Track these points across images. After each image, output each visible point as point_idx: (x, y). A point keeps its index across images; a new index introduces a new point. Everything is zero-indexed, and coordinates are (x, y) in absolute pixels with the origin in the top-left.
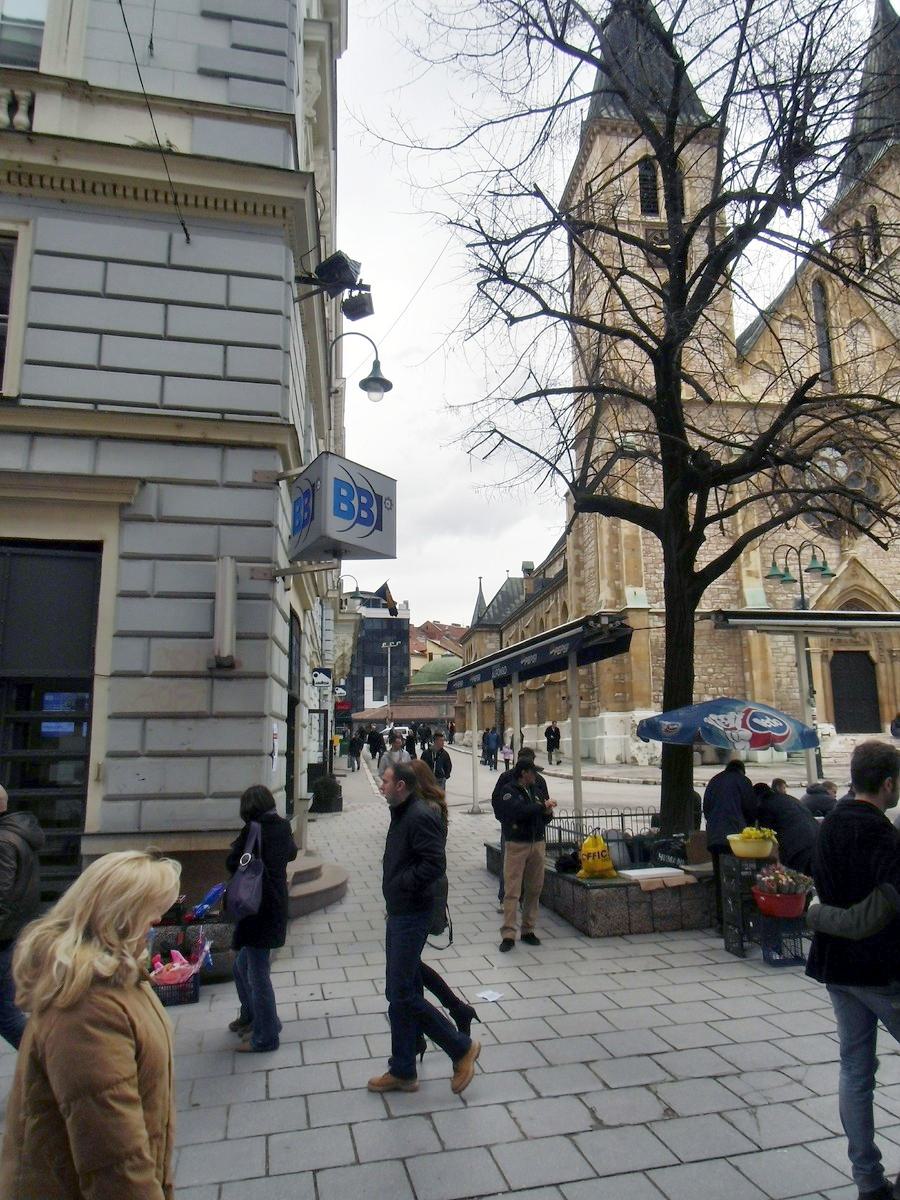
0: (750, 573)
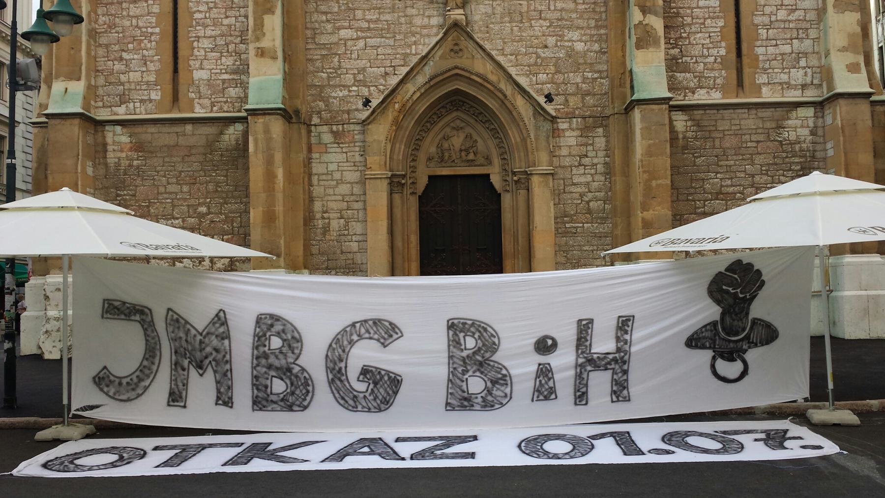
0: (262, 53)
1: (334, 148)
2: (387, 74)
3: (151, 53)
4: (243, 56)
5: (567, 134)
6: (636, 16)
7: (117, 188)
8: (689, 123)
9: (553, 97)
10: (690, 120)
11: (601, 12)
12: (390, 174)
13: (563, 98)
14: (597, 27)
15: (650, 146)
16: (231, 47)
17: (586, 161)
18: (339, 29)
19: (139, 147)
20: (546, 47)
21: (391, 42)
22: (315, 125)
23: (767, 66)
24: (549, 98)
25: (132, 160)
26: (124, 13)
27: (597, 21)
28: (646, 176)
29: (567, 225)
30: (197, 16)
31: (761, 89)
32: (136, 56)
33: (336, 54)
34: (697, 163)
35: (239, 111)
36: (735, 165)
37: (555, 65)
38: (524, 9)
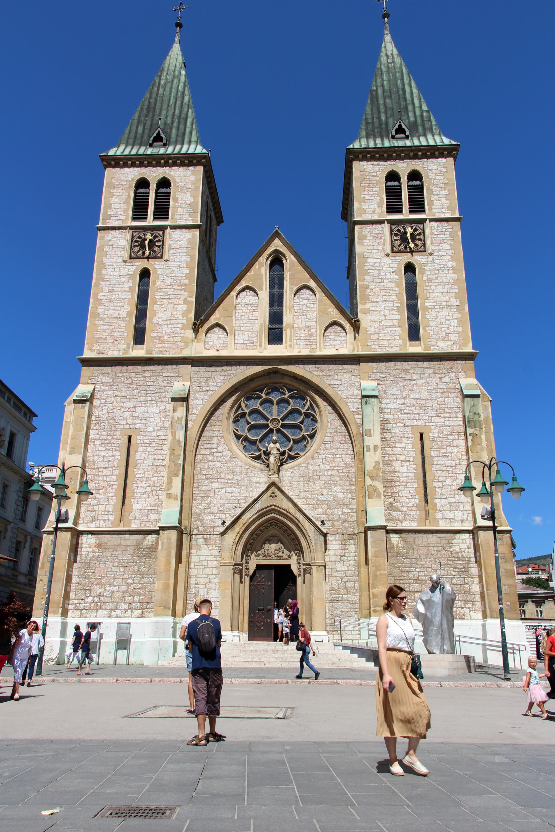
0: (169, 496)
1: (204, 548)
2: (236, 507)
3: (112, 495)
4: (160, 497)
5: (334, 542)
6: (368, 481)
7: (85, 568)
8: (400, 539)
9: (325, 522)
10: (400, 537)
11: (352, 477)
12: (234, 563)
13: (332, 522)
14: (350, 485)
15: (376, 551)
16: (154, 492)
17: (343, 558)
18: (212, 483)
19: (99, 546)
20: (322, 495)
21: (239, 490)
22: (195, 535)
23: (441, 509)
24: (323, 523)
25: (95, 552)
26: (100, 474)
27: (350, 482)
28: (374, 569)
29: (334, 596)
30: (138, 476)
31: (438, 521)
32: (103, 497)
33: (209, 496)
34: (405, 562)
35: (155, 527)
36: (426, 564)
37: (327, 504)
38: (311, 474)
